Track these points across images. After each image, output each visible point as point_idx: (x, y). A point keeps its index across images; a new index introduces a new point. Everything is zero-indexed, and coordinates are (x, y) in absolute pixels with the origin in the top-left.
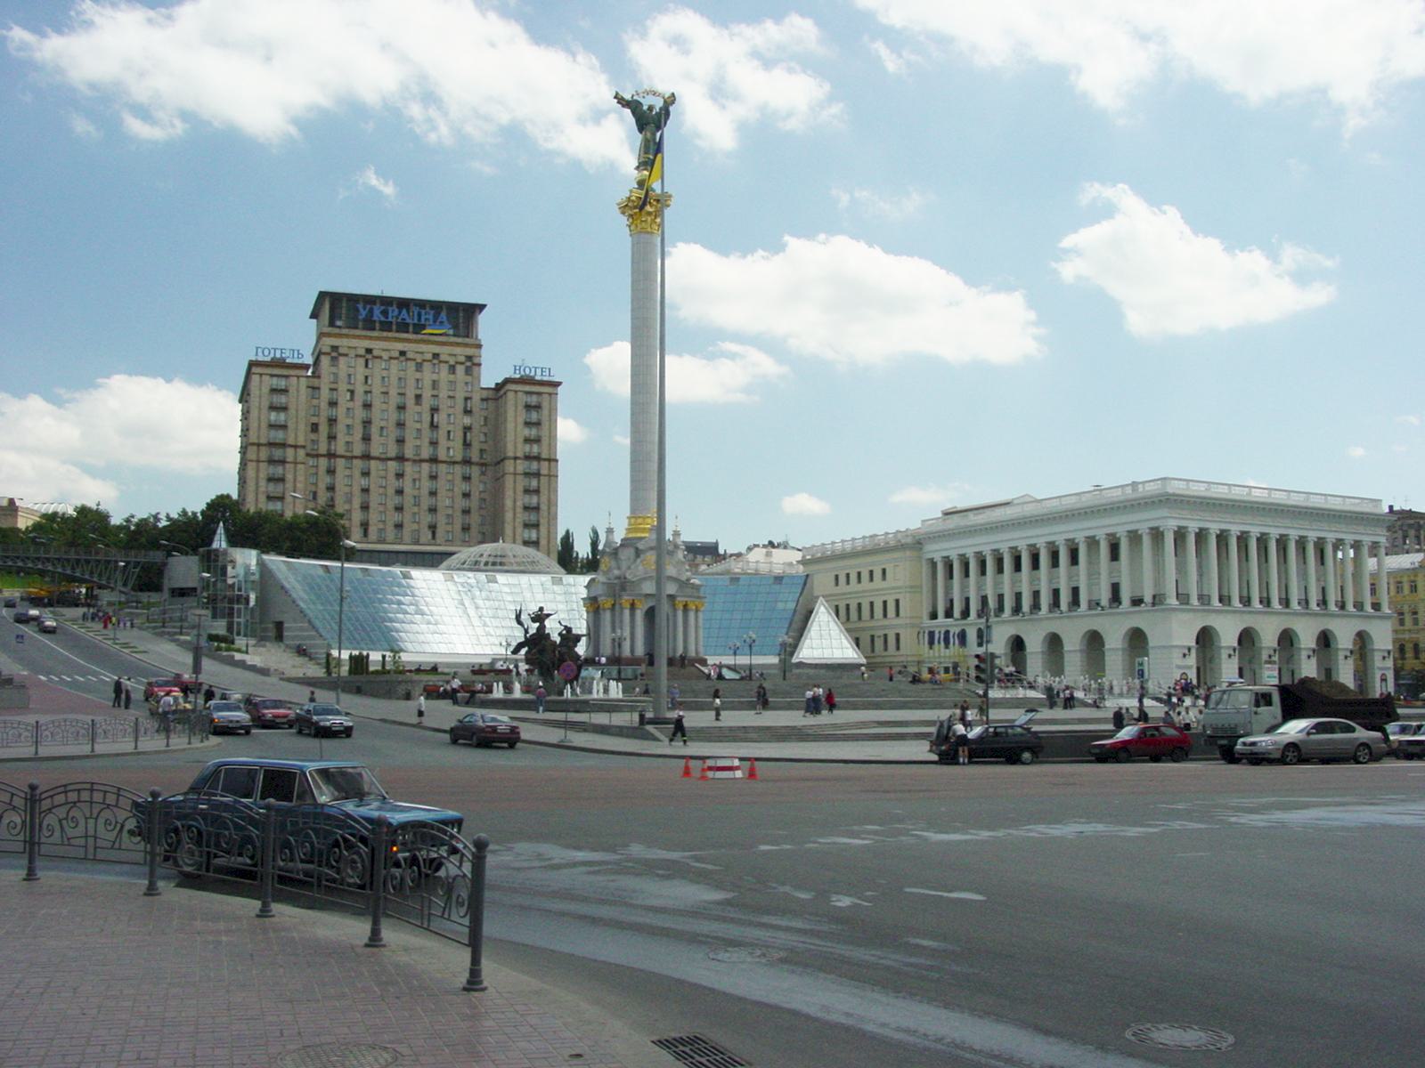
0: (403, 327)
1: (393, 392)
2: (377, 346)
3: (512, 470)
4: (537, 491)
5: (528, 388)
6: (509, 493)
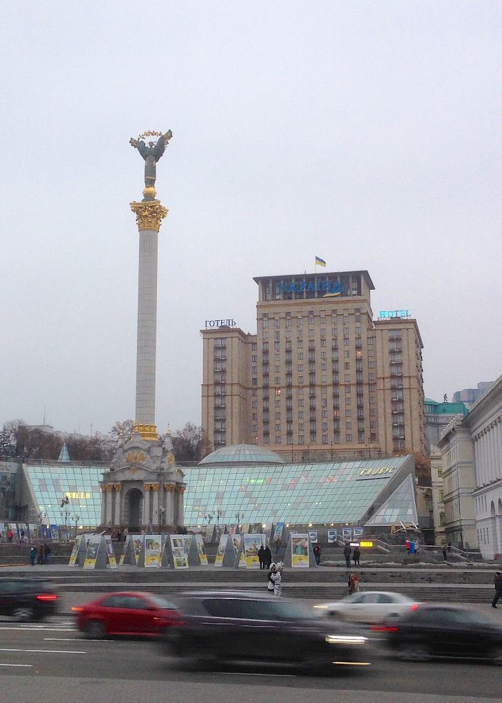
0: (310, 294)
1: (306, 340)
2: (293, 310)
3: (381, 387)
4: (401, 401)
5: (390, 327)
6: (381, 404)
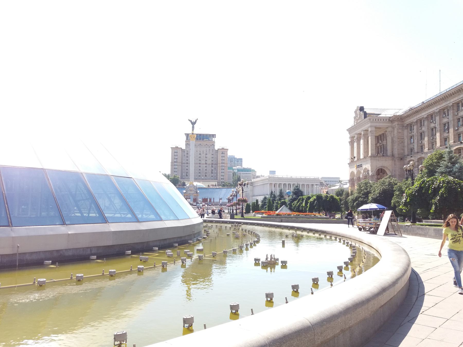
6: (218, 170)
